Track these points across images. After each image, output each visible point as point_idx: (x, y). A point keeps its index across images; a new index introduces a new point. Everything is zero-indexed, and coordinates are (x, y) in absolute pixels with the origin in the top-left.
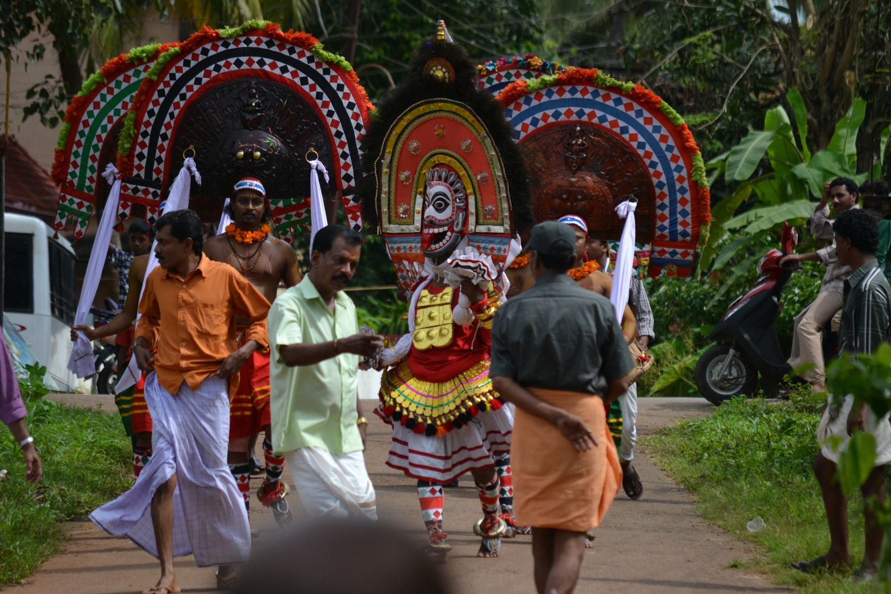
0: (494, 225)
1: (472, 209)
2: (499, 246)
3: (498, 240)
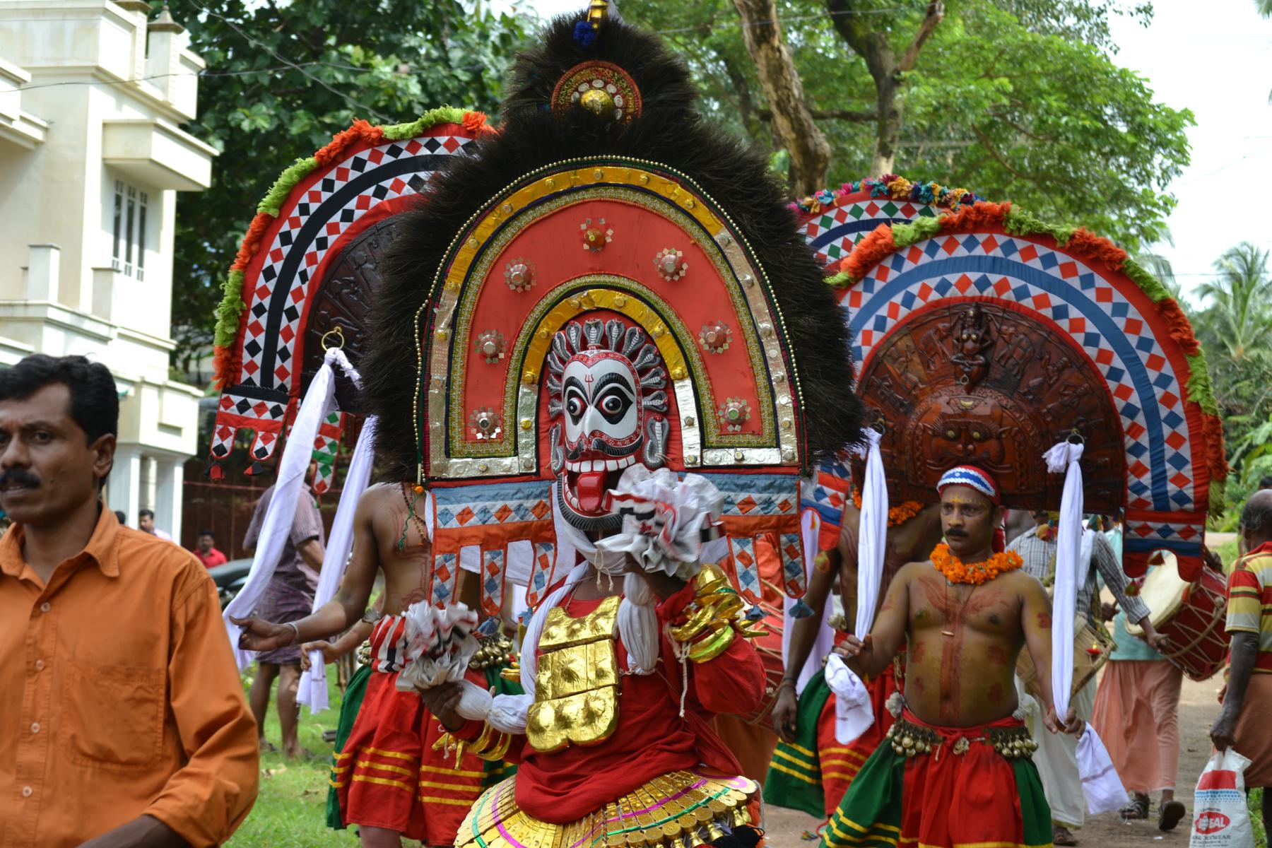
0: (750, 446)
1: (687, 408)
2: (765, 496)
3: (762, 481)
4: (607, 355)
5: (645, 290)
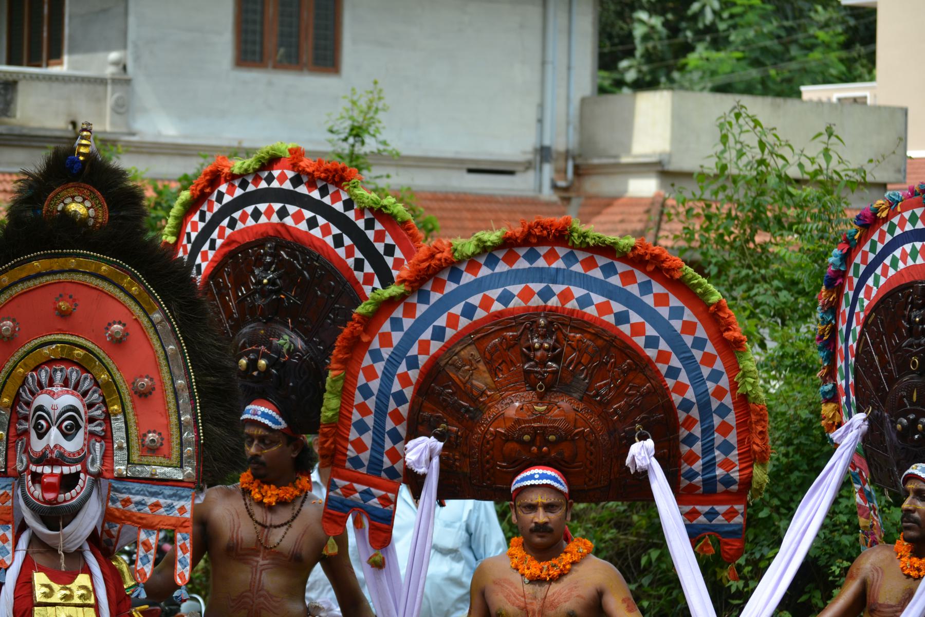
0: (161, 465)
1: (119, 437)
2: (169, 501)
3: (168, 491)
4: (68, 392)
5: (96, 348)
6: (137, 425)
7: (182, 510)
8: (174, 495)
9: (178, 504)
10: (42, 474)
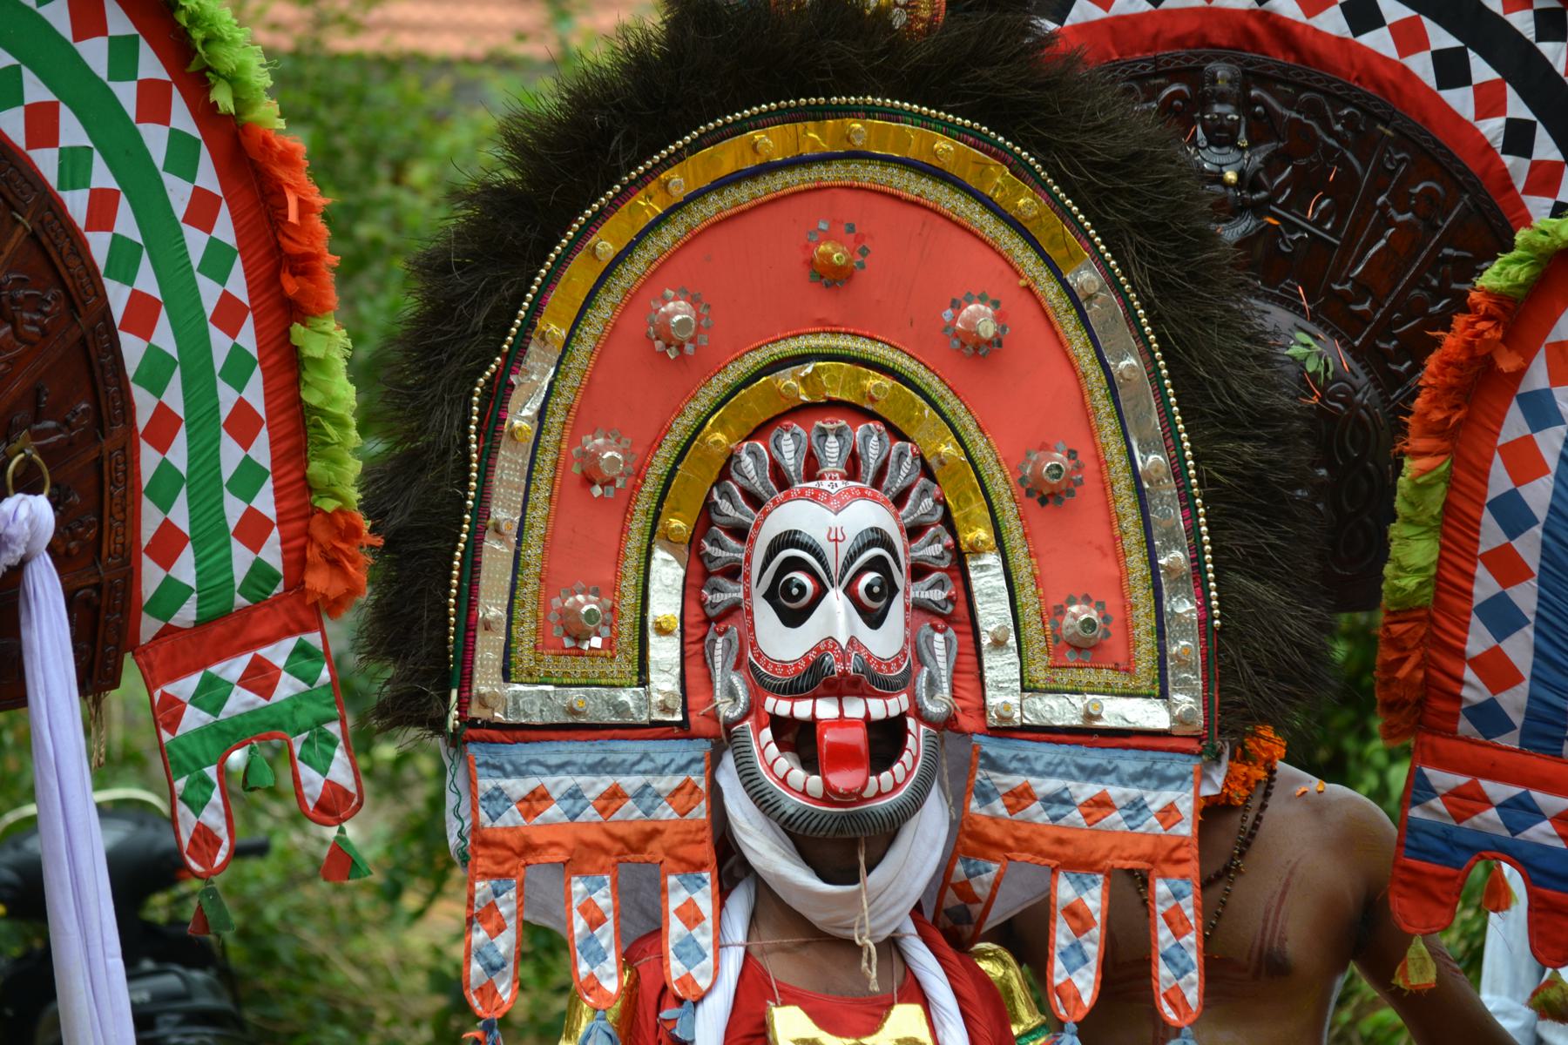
1: (993, 613)
6: (1038, 581)
7: (1168, 814)
8: (1146, 774)
9: (1158, 799)
10: (812, 724)
